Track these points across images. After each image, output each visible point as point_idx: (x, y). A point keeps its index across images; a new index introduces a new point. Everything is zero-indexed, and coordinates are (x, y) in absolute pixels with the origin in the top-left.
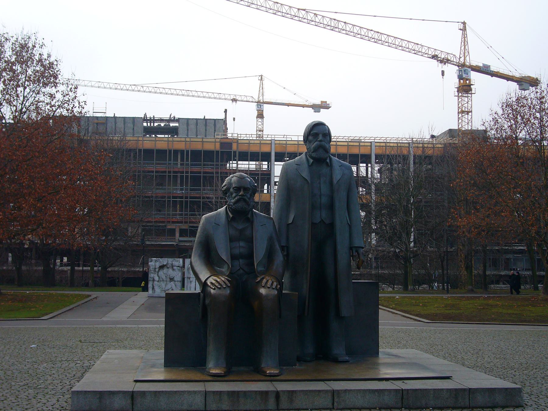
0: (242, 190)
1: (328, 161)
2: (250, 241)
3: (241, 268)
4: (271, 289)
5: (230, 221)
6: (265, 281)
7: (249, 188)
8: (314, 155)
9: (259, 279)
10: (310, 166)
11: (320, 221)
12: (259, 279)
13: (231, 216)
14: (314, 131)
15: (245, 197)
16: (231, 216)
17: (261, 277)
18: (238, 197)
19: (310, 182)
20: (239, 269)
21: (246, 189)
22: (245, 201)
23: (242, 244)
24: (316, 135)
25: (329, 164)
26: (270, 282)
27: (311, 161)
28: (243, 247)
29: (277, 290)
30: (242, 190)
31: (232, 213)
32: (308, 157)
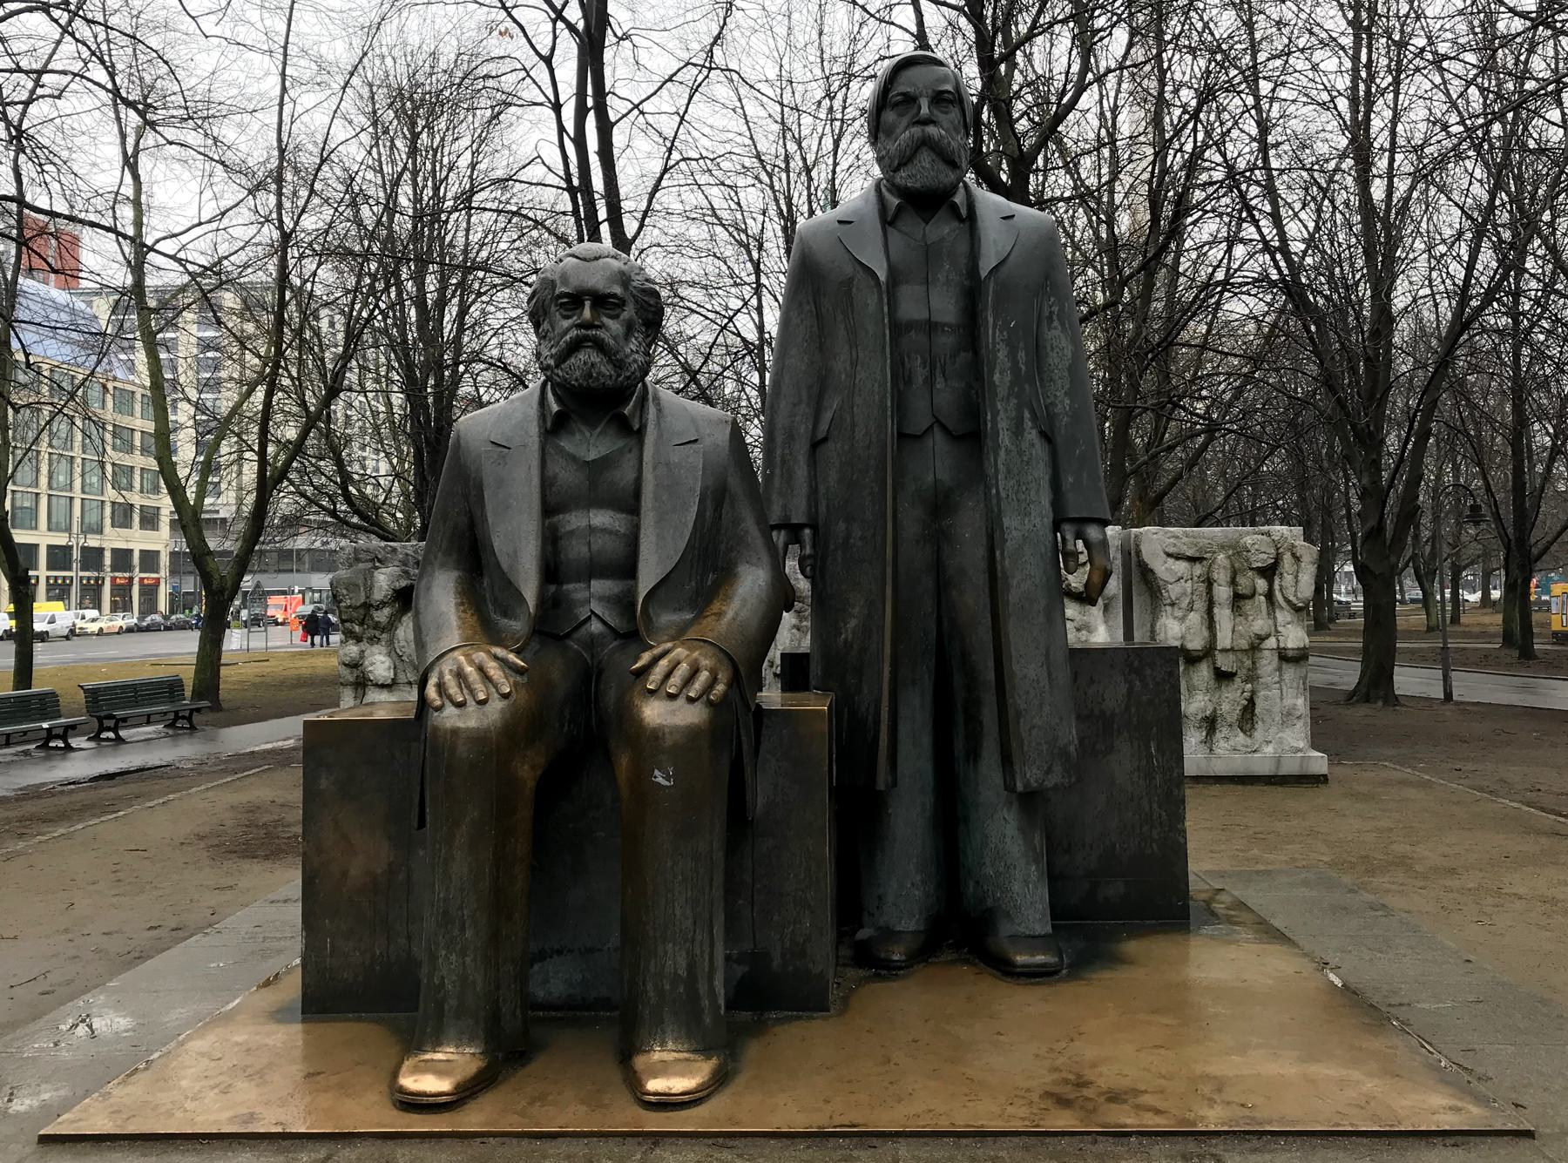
0: (588, 304)
1: (959, 198)
2: (630, 504)
3: (597, 616)
4: (681, 701)
5: (554, 427)
6: (664, 663)
7: (614, 296)
8: (902, 177)
9: (646, 657)
10: (888, 220)
11: (931, 427)
12: (646, 657)
13: (555, 408)
14: (902, 87)
15: (601, 333)
16: (555, 408)
17: (656, 651)
18: (574, 333)
19: (882, 276)
20: (589, 618)
21: (601, 301)
22: (600, 346)
23: (601, 518)
24: (910, 100)
25: (964, 212)
26: (684, 668)
27: (894, 201)
28: (604, 531)
29: (710, 703)
30: (588, 304)
31: (558, 399)
32: (883, 189)
